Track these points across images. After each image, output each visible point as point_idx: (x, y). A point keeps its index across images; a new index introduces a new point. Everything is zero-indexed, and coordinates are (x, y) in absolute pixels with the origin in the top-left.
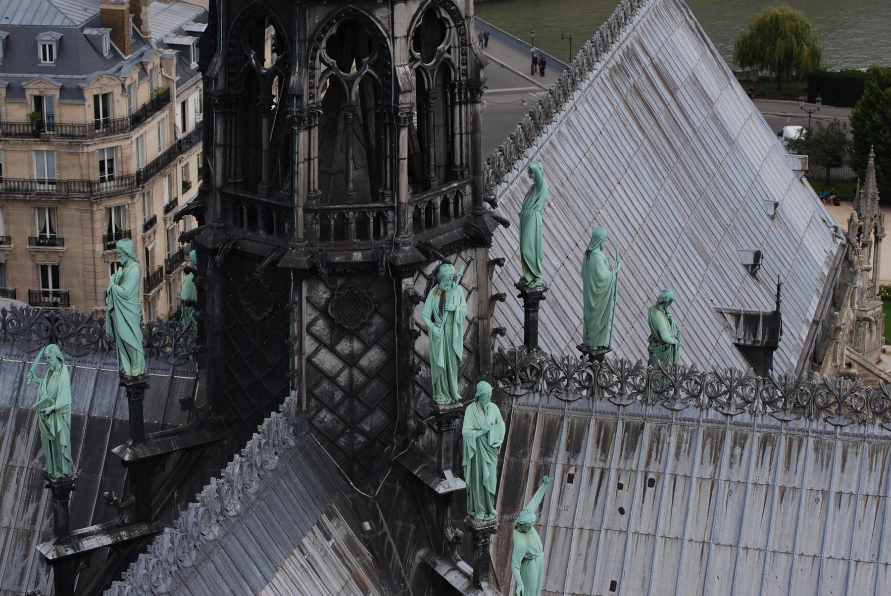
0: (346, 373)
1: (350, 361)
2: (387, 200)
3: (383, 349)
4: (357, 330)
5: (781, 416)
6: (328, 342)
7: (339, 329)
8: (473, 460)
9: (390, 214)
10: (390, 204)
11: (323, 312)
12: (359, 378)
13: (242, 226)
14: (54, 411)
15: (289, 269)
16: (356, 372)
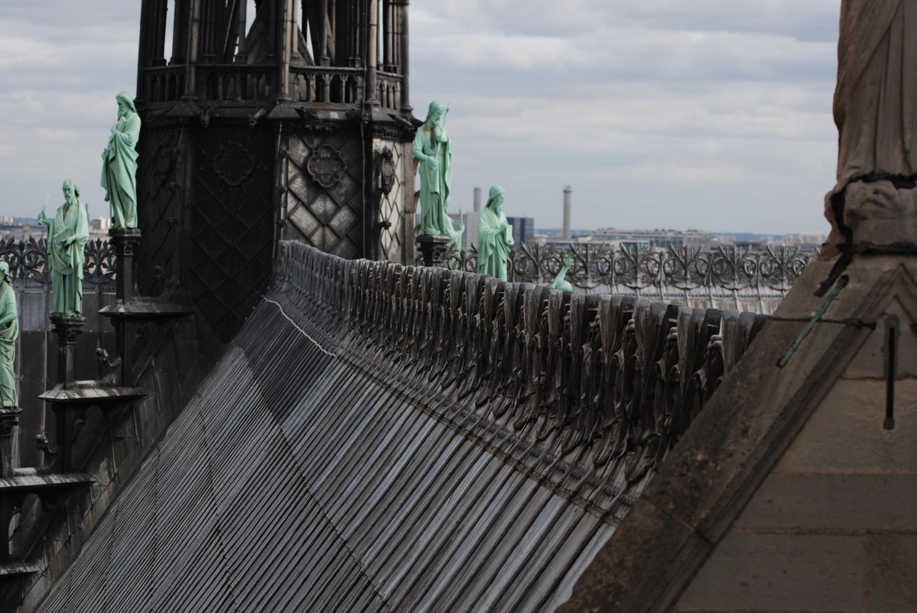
0: (319, 232)
1: (323, 221)
2: (357, 65)
3: (352, 210)
4: (329, 188)
5: (683, 285)
6: (305, 201)
7: (316, 188)
8: (491, 257)
9: (360, 80)
10: (361, 69)
11: (303, 170)
12: (331, 238)
13: (215, 97)
14: (74, 242)
15: (277, 120)
16: (328, 232)
